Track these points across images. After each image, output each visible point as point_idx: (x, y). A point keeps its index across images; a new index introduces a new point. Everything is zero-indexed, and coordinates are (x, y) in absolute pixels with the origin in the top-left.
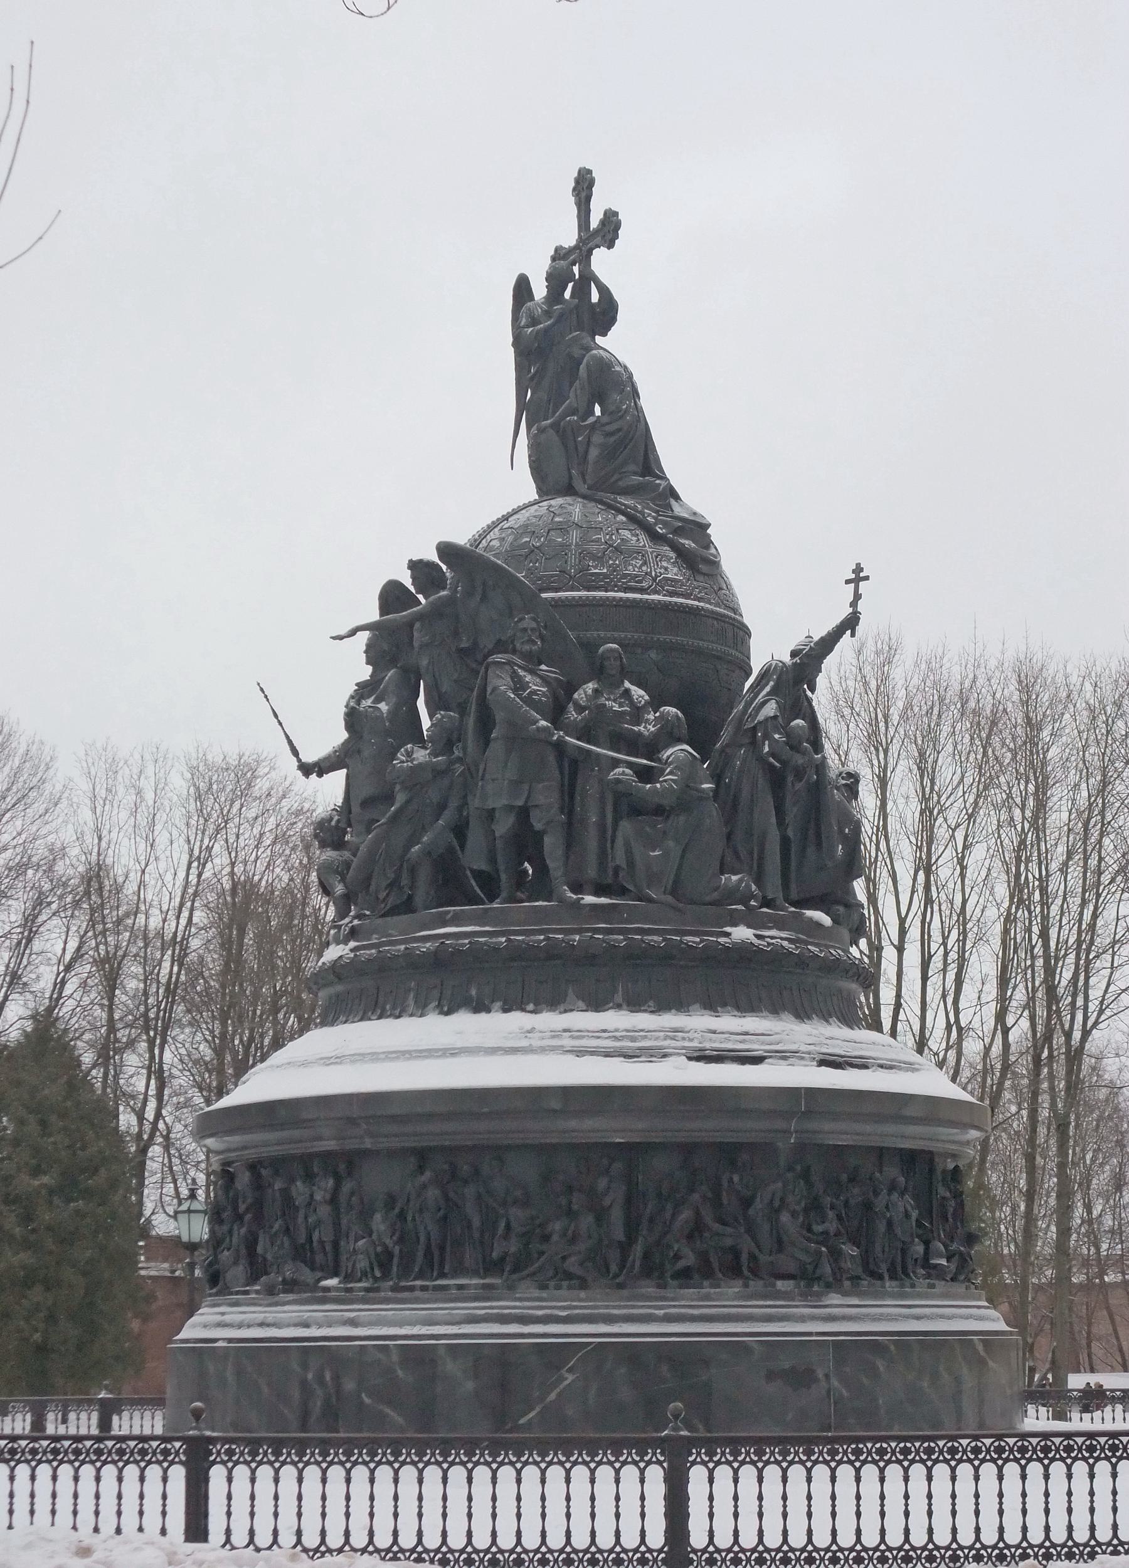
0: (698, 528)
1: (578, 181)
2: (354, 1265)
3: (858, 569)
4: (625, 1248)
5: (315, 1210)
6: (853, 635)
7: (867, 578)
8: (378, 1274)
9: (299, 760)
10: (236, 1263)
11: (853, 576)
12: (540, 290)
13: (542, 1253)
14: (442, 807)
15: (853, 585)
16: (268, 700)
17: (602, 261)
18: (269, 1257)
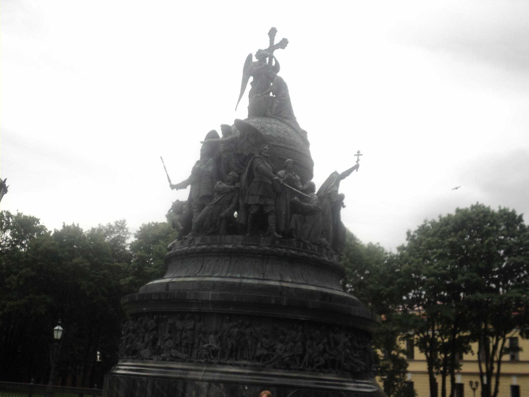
0: (305, 133)
1: (270, 31)
2: (201, 354)
3: (359, 152)
4: (302, 357)
5: (185, 332)
6: (357, 171)
7: (361, 155)
8: (212, 357)
9: (170, 184)
10: (146, 347)
11: (357, 154)
12: (255, 60)
13: (273, 356)
14: (230, 202)
15: (357, 157)
16: (163, 163)
17: (277, 53)
18: (162, 347)
